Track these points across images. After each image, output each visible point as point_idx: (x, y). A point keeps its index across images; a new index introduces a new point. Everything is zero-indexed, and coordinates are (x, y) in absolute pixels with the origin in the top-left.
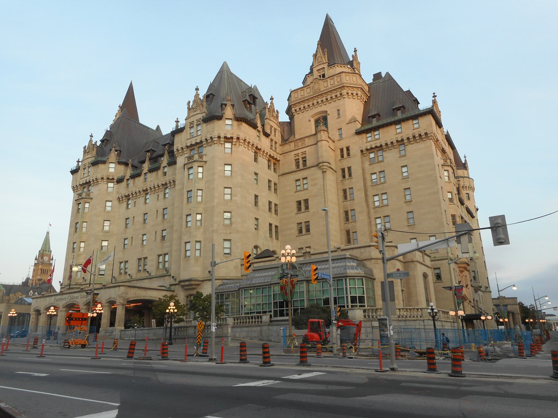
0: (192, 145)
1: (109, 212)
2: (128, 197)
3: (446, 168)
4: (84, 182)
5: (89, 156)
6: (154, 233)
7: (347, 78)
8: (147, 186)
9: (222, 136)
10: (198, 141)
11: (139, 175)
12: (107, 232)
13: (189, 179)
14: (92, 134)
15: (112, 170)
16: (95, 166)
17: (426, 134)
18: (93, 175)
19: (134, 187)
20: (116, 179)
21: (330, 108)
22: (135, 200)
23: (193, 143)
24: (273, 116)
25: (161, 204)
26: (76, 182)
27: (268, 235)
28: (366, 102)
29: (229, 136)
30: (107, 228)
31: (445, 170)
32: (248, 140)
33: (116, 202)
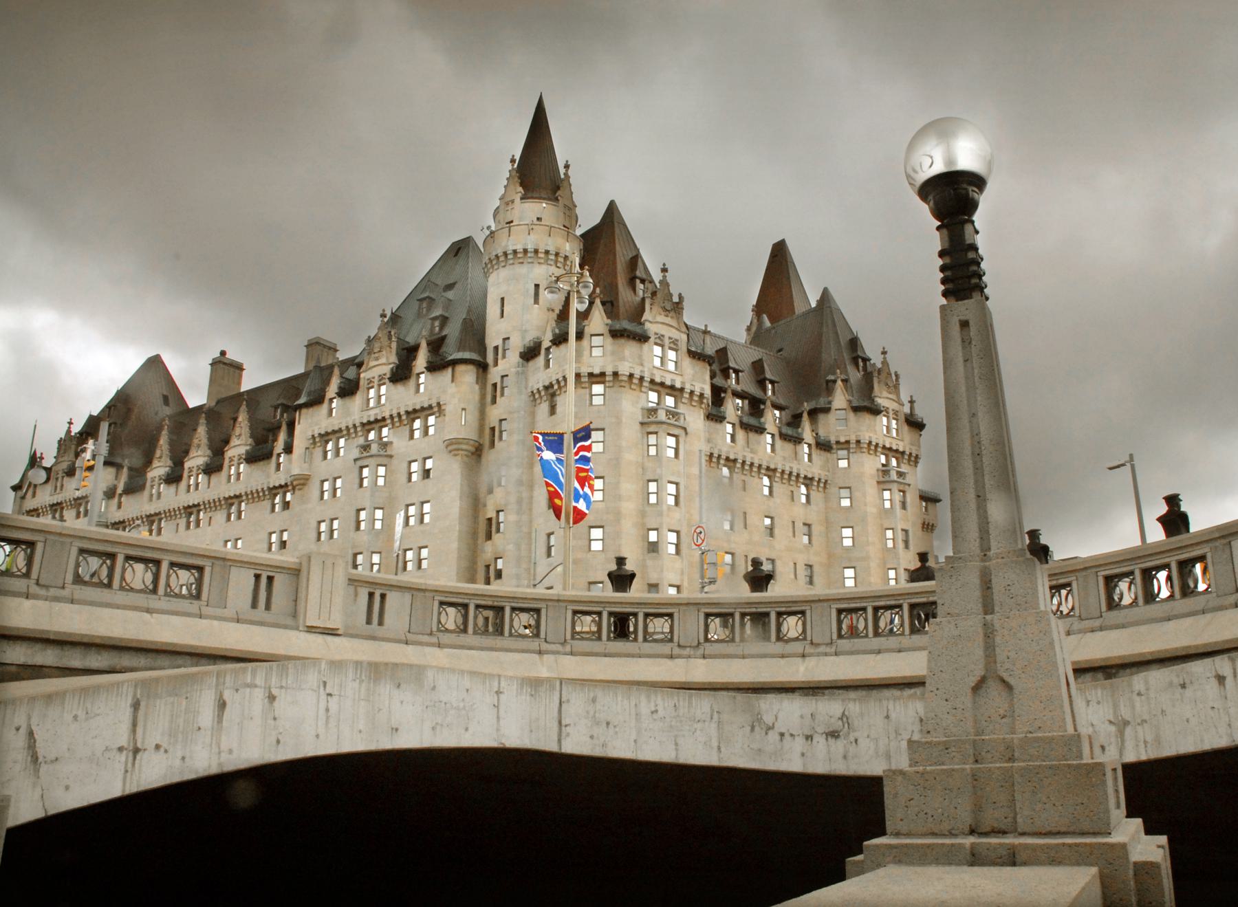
0: (890, 449)
2: (730, 462)
4: (668, 383)
5: (668, 320)
6: (792, 565)
8: (775, 464)
10: (901, 449)
11: (761, 430)
14: (664, 265)
16: (695, 361)
17: (933, 525)
18: (693, 380)
19: (749, 450)
22: (743, 477)
23: (894, 448)
25: (799, 512)
26: (641, 368)
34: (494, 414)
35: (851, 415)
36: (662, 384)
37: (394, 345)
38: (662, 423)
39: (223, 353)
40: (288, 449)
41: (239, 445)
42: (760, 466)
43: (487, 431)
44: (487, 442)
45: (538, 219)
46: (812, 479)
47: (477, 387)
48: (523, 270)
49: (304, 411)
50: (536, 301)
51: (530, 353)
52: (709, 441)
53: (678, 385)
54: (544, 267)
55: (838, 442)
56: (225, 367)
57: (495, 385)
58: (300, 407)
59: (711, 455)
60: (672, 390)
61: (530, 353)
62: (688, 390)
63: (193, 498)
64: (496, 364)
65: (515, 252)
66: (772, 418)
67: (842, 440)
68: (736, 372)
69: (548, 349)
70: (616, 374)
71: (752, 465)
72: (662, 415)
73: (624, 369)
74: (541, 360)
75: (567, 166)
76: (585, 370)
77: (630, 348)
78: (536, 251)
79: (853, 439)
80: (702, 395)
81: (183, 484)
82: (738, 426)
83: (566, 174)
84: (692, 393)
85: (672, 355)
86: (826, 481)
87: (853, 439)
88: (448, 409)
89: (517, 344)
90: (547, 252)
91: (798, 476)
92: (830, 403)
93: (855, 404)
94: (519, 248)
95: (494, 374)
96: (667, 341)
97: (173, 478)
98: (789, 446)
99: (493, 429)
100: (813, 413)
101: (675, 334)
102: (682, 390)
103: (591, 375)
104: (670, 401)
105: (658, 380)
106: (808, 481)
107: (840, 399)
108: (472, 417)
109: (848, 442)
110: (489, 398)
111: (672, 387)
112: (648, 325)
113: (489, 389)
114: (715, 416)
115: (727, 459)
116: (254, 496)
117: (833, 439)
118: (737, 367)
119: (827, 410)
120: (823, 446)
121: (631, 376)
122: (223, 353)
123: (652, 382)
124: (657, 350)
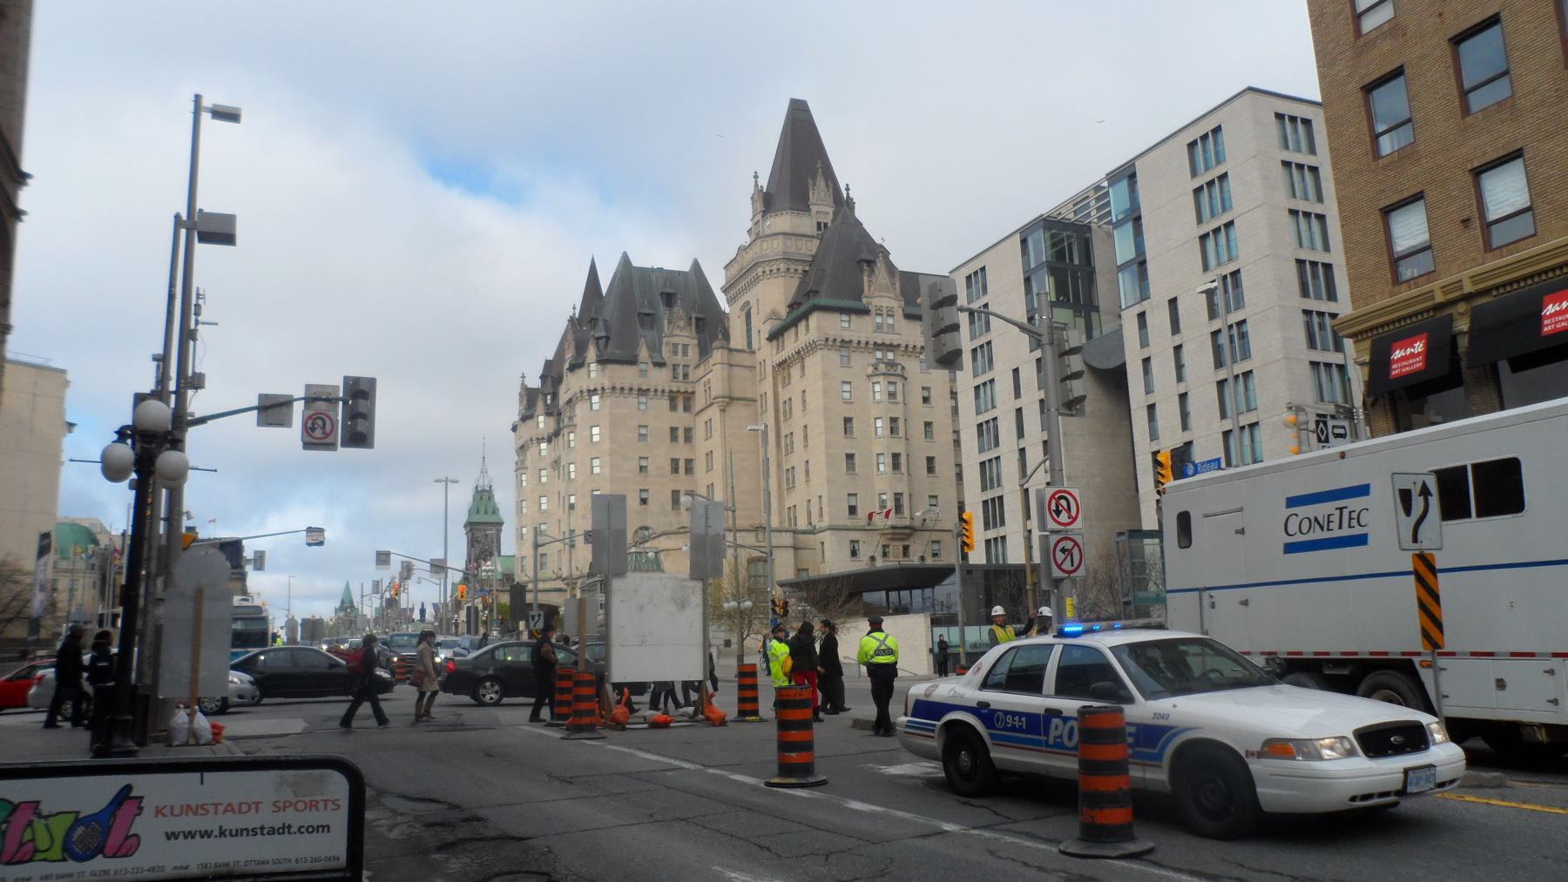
1: (544, 484)
3: (875, 379)
7: (765, 245)
9: (585, 389)
12: (544, 512)
13: (569, 447)
15: (541, 425)
20: (546, 437)
21: (749, 296)
24: (678, 326)
27: (669, 507)
28: (805, 271)
29: (592, 388)
30: (544, 507)
31: (874, 383)
32: (618, 385)
33: (550, 469)
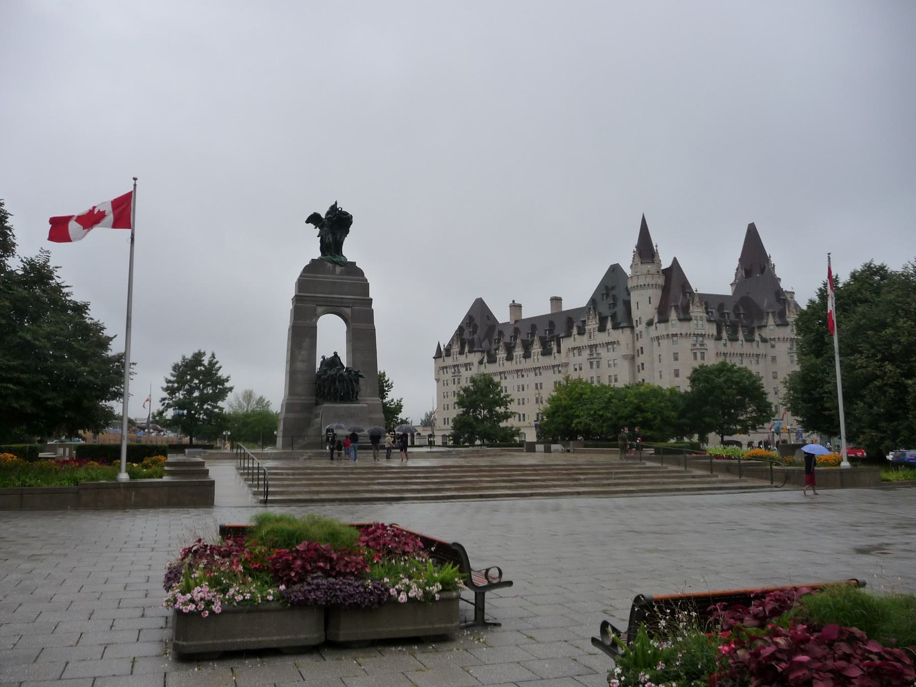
11: (737, 340)
34: (639, 345)
35: (776, 328)
36: (698, 334)
37: (597, 317)
38: (698, 349)
39: (514, 301)
40: (559, 352)
41: (536, 349)
42: (737, 354)
43: (636, 351)
44: (636, 355)
45: (648, 271)
46: (759, 355)
47: (631, 335)
48: (643, 292)
49: (564, 339)
50: (650, 303)
51: (650, 323)
52: (716, 348)
53: (703, 333)
54: (652, 290)
55: (770, 339)
56: (516, 307)
57: (637, 334)
58: (562, 337)
59: (717, 353)
60: (702, 335)
61: (650, 323)
62: (707, 333)
63: (519, 367)
64: (637, 326)
65: (641, 285)
66: (741, 336)
67: (772, 338)
68: (728, 313)
69: (656, 323)
70: (681, 334)
71: (734, 354)
72: (698, 346)
73: (684, 332)
74: (654, 327)
75: (656, 246)
76: (670, 333)
77: (686, 324)
78: (648, 285)
79: (777, 337)
80: (712, 335)
81: (514, 362)
82: (728, 341)
83: (657, 250)
84: (709, 335)
85: (700, 322)
86: (765, 355)
87: (777, 337)
88: (621, 343)
89: (645, 320)
90: (652, 285)
91: (753, 354)
92: (767, 323)
93: (777, 323)
94: (642, 284)
95: (637, 330)
96: (698, 318)
97: (510, 358)
98: (749, 344)
99: (638, 350)
100: (760, 327)
101: (702, 314)
102: (705, 335)
103: (672, 334)
104: (701, 339)
105: (696, 333)
106: (758, 356)
107: (771, 321)
108: (630, 346)
109: (774, 339)
110: (636, 338)
111: (702, 334)
112: (691, 314)
113: (635, 335)
114: (719, 338)
115: (724, 353)
116: (546, 368)
117: (768, 338)
118: (727, 311)
119: (765, 326)
120: (764, 340)
121: (687, 334)
122: (514, 301)
123: (694, 334)
124: (695, 322)
